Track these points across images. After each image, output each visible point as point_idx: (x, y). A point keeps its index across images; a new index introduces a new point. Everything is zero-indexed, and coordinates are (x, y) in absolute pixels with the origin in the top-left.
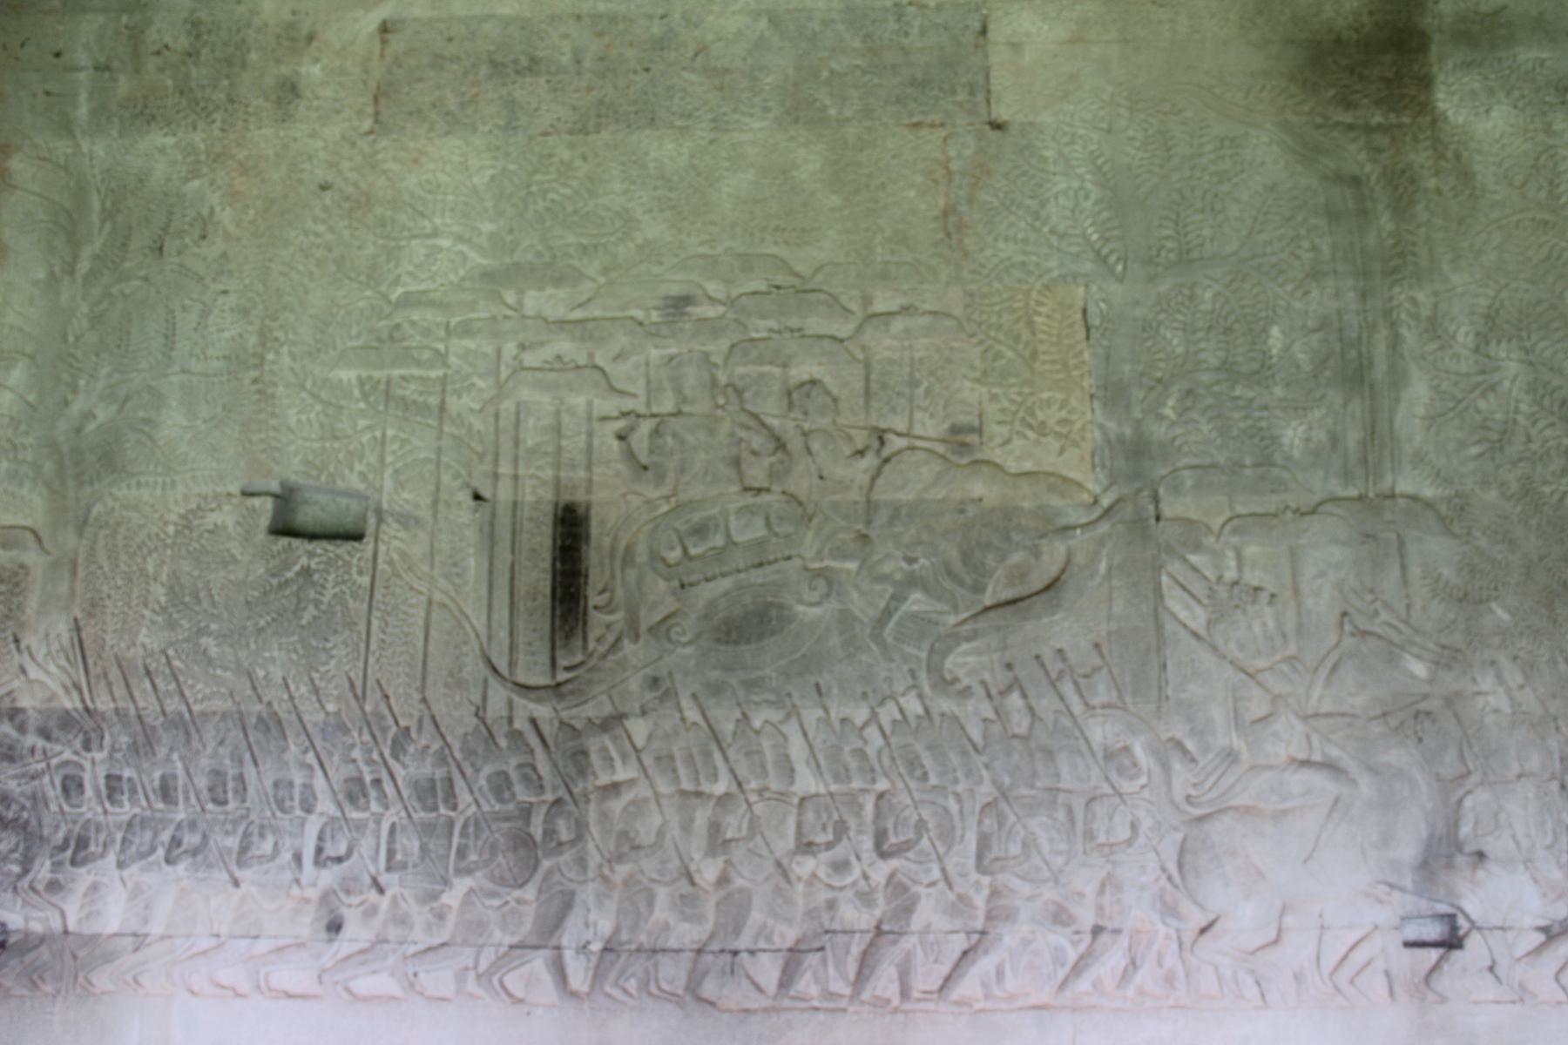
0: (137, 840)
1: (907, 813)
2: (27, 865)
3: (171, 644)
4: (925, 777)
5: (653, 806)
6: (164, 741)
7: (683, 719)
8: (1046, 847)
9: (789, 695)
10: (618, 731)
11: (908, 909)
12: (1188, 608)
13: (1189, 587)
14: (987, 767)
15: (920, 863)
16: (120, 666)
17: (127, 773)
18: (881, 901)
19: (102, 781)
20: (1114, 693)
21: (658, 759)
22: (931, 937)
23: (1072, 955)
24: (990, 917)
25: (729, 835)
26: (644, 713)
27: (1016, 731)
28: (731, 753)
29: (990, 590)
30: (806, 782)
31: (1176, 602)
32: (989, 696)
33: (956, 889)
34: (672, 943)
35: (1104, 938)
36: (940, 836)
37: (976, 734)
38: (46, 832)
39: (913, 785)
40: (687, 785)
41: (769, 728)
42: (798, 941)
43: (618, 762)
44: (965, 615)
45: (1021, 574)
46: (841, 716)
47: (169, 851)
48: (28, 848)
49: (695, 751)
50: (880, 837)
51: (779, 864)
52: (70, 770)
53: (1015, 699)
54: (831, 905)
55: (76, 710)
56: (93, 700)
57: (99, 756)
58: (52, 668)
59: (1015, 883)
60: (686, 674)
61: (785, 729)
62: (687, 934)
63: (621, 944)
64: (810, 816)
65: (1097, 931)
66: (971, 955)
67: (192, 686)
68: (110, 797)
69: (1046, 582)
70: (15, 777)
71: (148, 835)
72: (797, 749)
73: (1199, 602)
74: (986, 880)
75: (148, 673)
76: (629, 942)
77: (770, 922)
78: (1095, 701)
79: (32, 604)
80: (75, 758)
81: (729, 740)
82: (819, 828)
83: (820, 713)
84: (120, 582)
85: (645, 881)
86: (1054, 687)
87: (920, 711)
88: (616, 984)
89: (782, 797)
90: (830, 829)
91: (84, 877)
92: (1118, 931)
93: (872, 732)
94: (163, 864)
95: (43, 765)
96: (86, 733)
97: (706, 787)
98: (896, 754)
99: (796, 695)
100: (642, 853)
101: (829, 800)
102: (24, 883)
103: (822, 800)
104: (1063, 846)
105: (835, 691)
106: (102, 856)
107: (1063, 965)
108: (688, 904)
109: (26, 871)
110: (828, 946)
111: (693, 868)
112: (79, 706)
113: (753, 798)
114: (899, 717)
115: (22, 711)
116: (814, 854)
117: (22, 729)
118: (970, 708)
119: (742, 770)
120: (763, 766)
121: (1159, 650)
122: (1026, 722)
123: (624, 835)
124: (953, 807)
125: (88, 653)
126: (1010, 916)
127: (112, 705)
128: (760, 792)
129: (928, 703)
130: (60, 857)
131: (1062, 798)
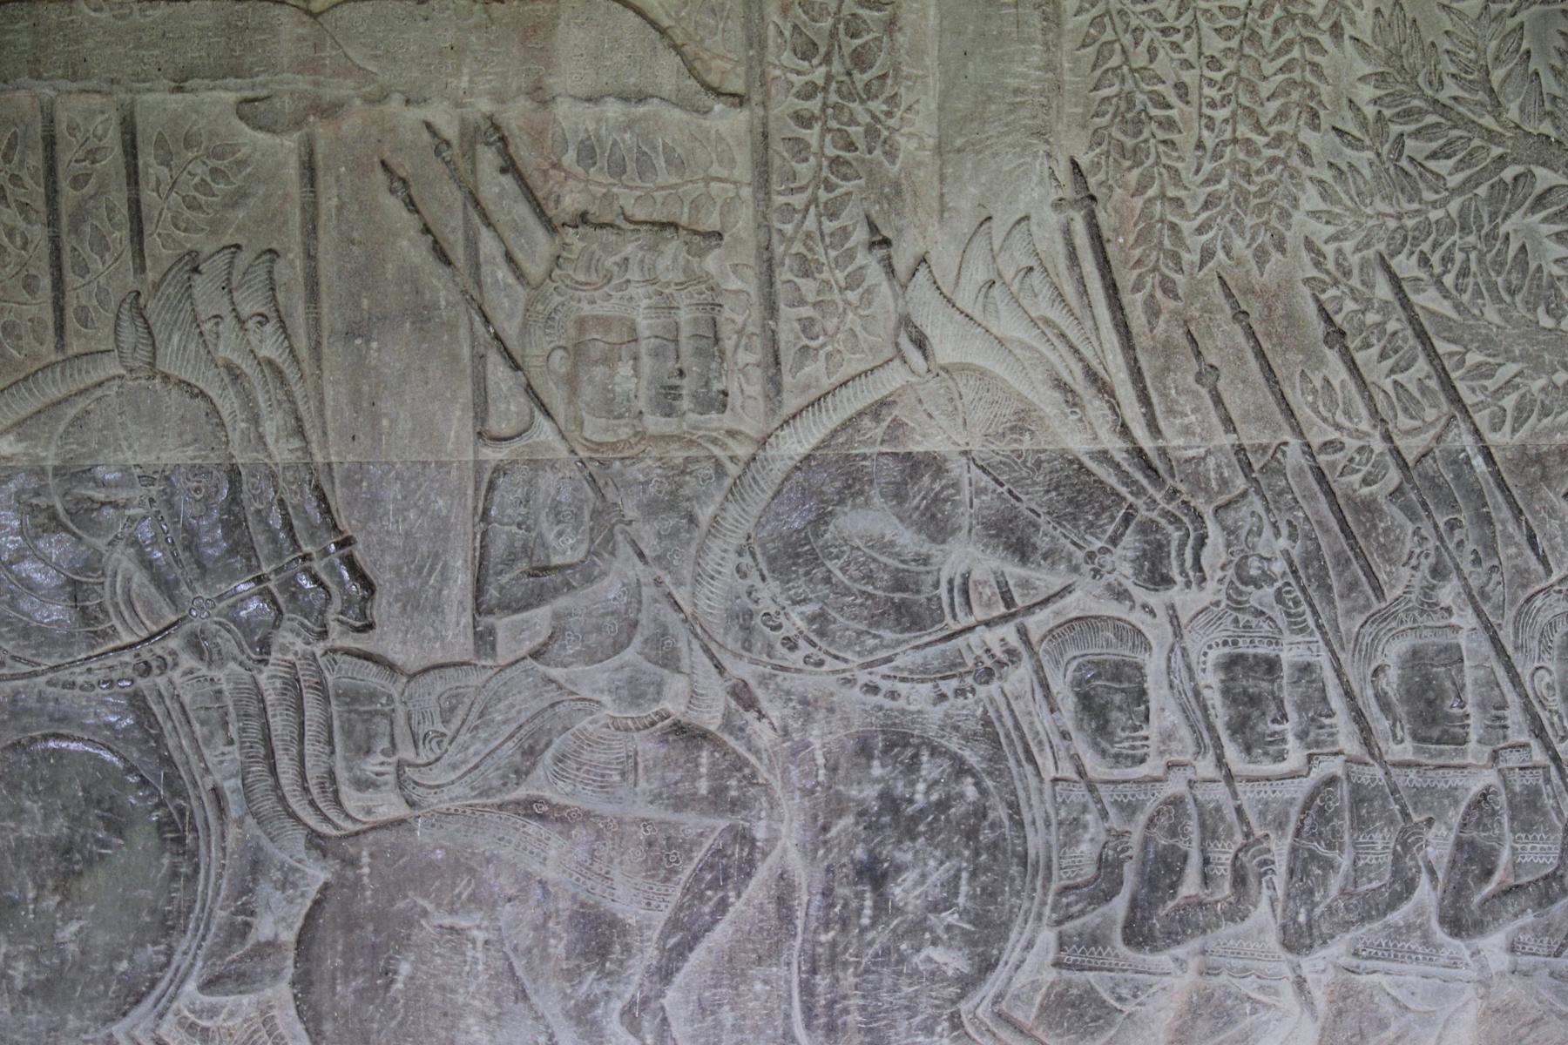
0: (1344, 862)
2: (985, 941)
3: (1403, 240)
6: (1410, 543)
16: (1240, 315)
17: (1290, 653)
19: (1211, 680)
38: (1035, 843)
47: (1457, 892)
48: (990, 894)
52: (1106, 649)
55: (1104, 456)
56: (1154, 429)
57: (1186, 599)
58: (1010, 326)
67: (1482, 372)
68: (1239, 727)
70: (921, 674)
71: (1382, 841)
75: (1336, 336)
79: (916, 131)
80: (1113, 609)
84: (1215, 45)
91: (1171, 976)
94: (1440, 934)
95: (1008, 632)
96: (1147, 528)
102: (978, 1006)
106: (1236, 913)
109: (987, 966)
112: (1116, 446)
115: (934, 464)
117: (936, 524)
125: (1126, 278)
127: (1227, 441)
130: (1093, 918)
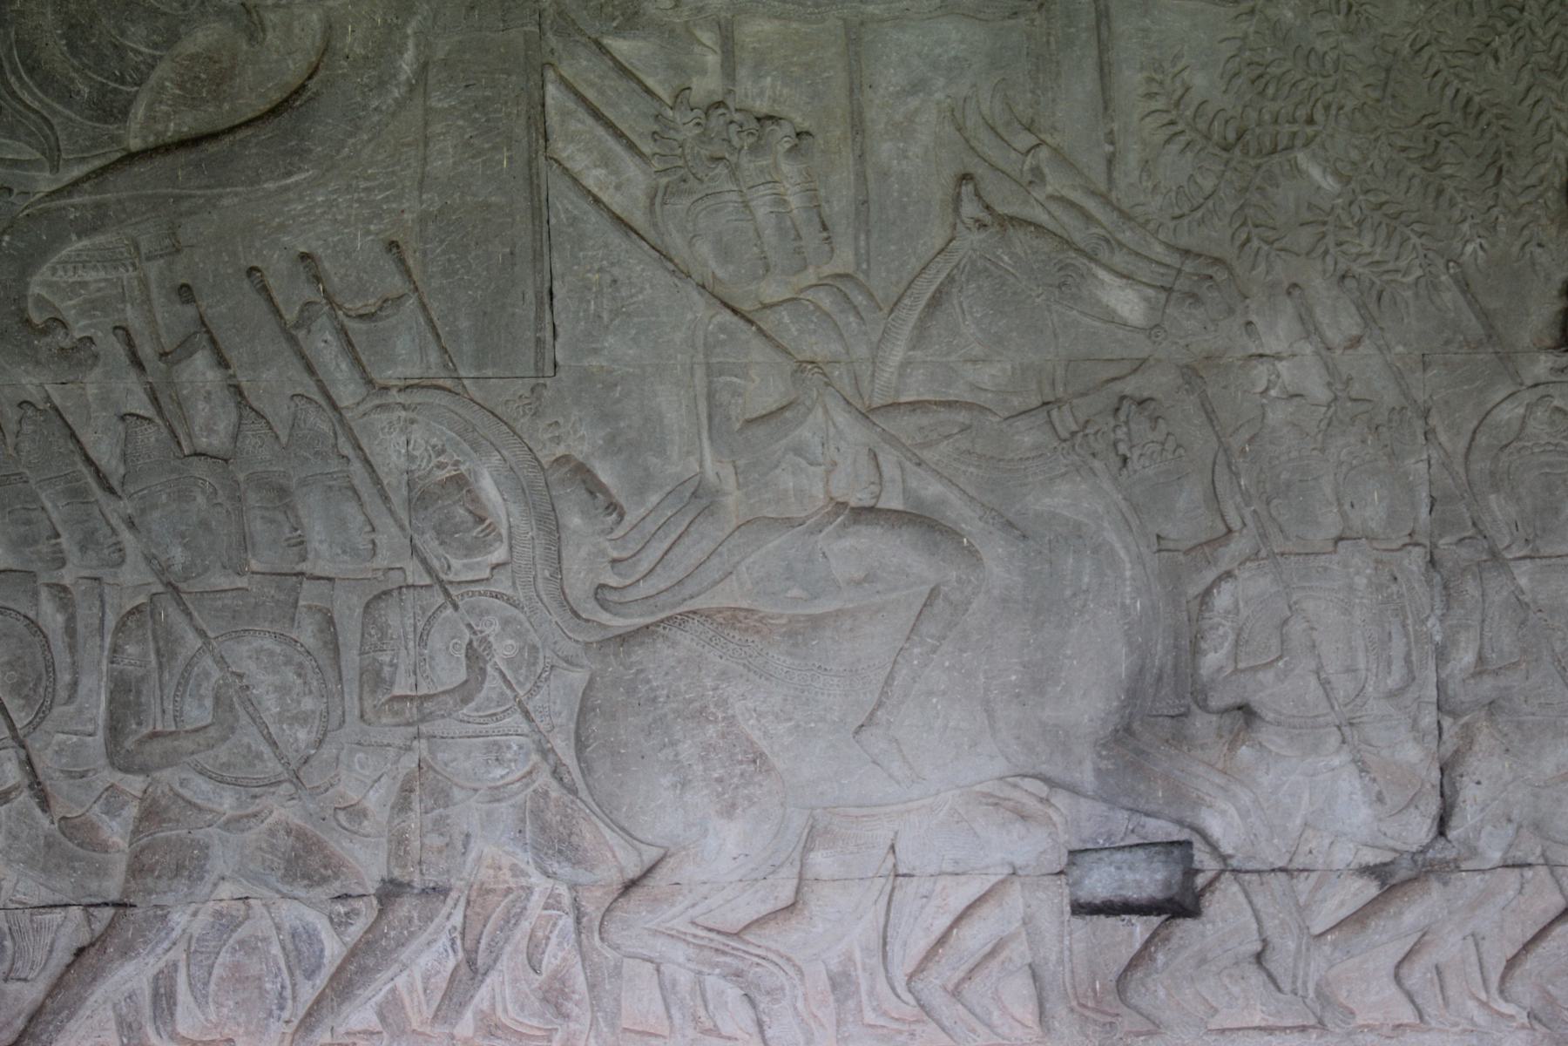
12: (606, 161)
13: (610, 114)
14: (131, 524)
20: (434, 356)
23: (333, 948)
24: (137, 869)
27: (203, 442)
29: (139, 111)
31: (578, 148)
32: (137, 363)
33: (59, 810)
35: (406, 907)
37: (105, 452)
44: (77, 172)
45: (215, 75)
53: (200, 369)
59: (200, 789)
65: (391, 891)
66: (90, 958)
69: (276, 97)
73: (631, 146)
74: (135, 784)
78: (388, 374)
86: (292, 340)
92: (440, 892)
104: (308, 704)
107: (310, 975)
121: (537, 256)
122: (224, 425)
124: (51, 617)
126: (188, 865)
131: (309, 594)
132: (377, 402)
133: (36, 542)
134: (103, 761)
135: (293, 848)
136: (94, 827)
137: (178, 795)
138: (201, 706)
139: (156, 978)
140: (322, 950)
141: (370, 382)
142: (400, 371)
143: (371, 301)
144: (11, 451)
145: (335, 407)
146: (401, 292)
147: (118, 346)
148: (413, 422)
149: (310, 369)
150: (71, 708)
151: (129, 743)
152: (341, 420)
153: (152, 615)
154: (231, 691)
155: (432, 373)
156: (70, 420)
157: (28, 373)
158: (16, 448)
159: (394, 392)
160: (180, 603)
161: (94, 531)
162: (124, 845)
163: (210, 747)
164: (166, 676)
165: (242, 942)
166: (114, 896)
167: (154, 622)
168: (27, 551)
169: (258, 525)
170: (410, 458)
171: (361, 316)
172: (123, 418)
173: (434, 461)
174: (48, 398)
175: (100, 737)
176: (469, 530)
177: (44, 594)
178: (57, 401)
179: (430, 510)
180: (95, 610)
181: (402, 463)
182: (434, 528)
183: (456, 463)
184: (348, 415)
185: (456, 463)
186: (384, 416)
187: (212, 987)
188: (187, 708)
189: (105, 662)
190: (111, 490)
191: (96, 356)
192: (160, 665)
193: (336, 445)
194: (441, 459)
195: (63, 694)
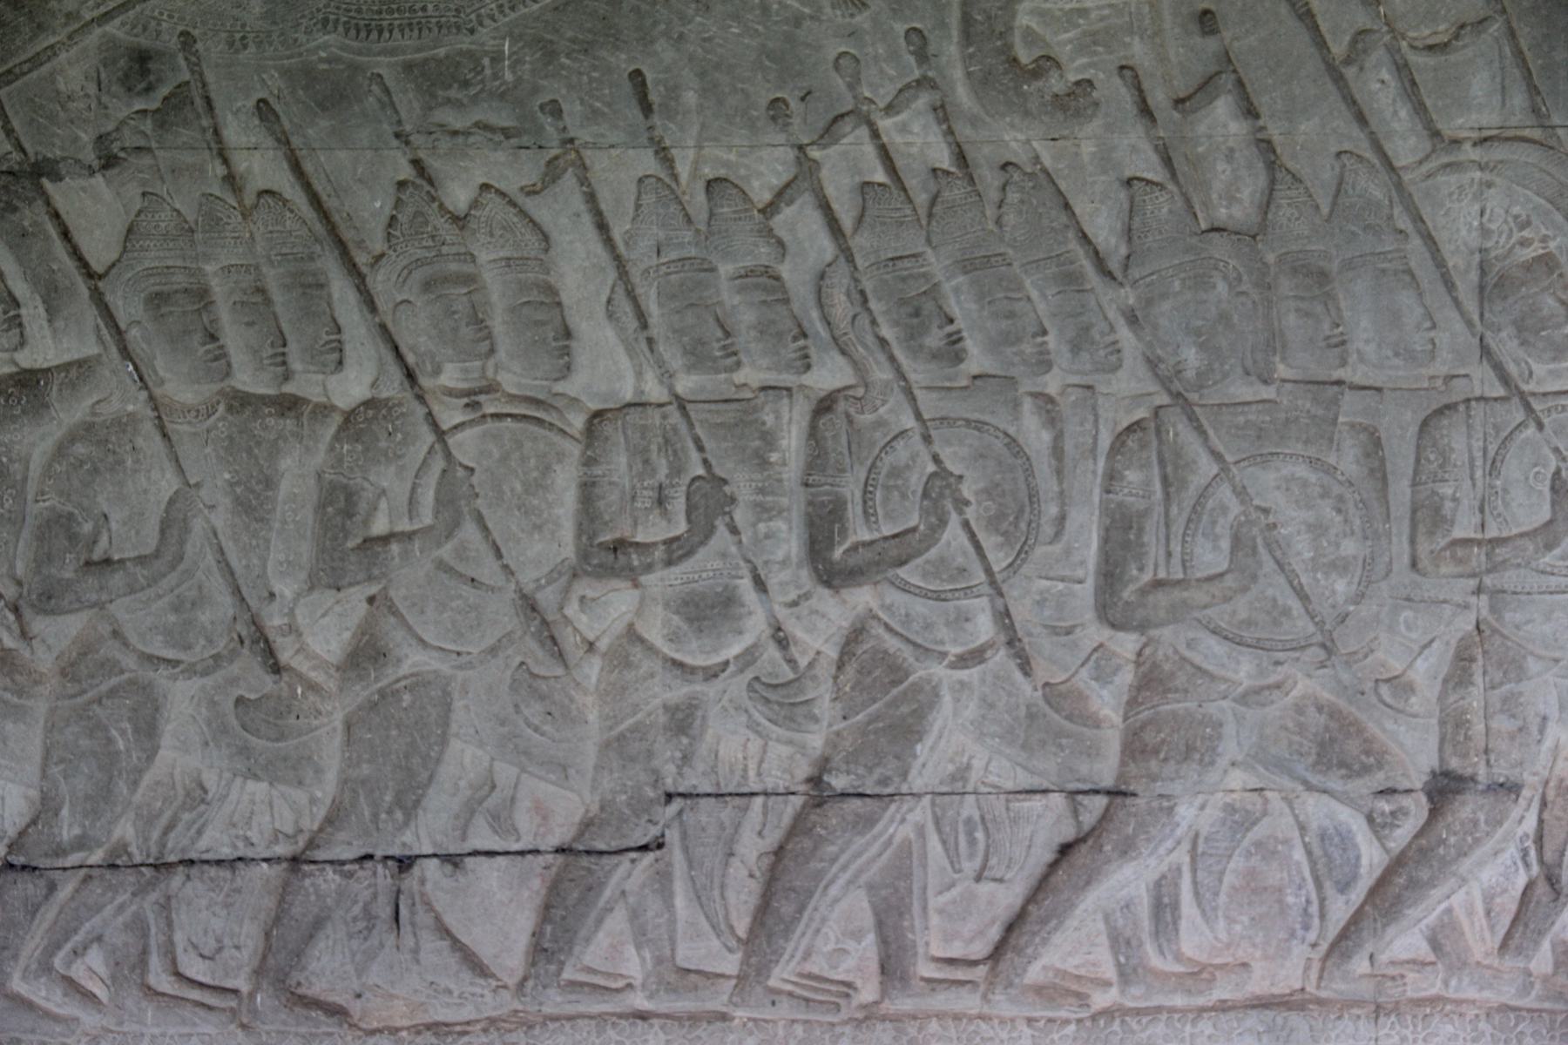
1: (901, 453)
4: (953, 350)
5: (150, 441)
7: (231, 180)
8: (1302, 549)
9: (555, 110)
10: (31, 215)
11: (905, 730)
14: (1132, 319)
15: (938, 596)
18: (825, 707)
20: (1519, 100)
21: (158, 301)
22: (969, 808)
23: (1371, 857)
24: (1135, 747)
25: (380, 526)
26: (109, 162)
28: (380, 282)
30: (607, 368)
32: (1146, 111)
33: (1042, 672)
34: (216, 841)
35: (1467, 808)
36: (994, 523)
37: (1104, 228)
39: (919, 373)
40: (248, 379)
41: (493, 207)
42: (587, 825)
43: (33, 312)
46: (708, 172)
49: (272, 278)
50: (822, 526)
51: (529, 605)
53: (1221, 119)
54: (683, 720)
60: (236, 44)
61: (541, 210)
62: (260, 813)
63: (60, 852)
64: (618, 465)
65: (1445, 788)
72: (579, 270)
74: (1126, 644)
76: (81, 843)
77: (505, 773)
78: (1458, 124)
81: (378, 246)
82: (645, 499)
83: (647, 163)
85: (129, 661)
86: (1339, 80)
87: (944, 159)
88: (46, 968)
89: (536, 411)
90: (678, 505)
92: (1511, 789)
93: (801, 223)
97: (307, 384)
98: (868, 285)
99: (573, 109)
100: (117, 580)
101: (675, 417)
103: (655, 417)
104: (1349, 547)
105: (690, 98)
107: (1344, 887)
108: (261, 727)
110: (672, 836)
111: (274, 621)
113: (450, 415)
114: (880, 176)
116: (632, 576)
118: (1088, 148)
119: (416, 335)
120: (478, 321)
122: (1251, 188)
123: (59, 527)
124: (1035, 434)
126: (1197, 747)
128: (471, 398)
129: (964, 131)
131: (1351, 408)
132: (1446, 159)
133: (1019, 340)
134: (1090, 615)
135: (1327, 728)
136: (1081, 697)
137: (1184, 659)
138: (1216, 548)
139: (1158, 884)
140: (1358, 858)
141: (1435, 134)
142: (1475, 119)
143: (1442, 28)
144: (991, 226)
145: (1390, 167)
146: (1482, 14)
147: (1123, 90)
148: (1489, 185)
149: (1361, 119)
150: (1057, 548)
151: (1128, 594)
152: (1399, 186)
153: (1158, 432)
154: (1255, 531)
155: (1514, 121)
156: (1063, 185)
157: (1012, 126)
158: (998, 222)
159: (1467, 146)
160: (1192, 418)
161: (1087, 329)
162: (1117, 719)
163: (1227, 599)
164: (1174, 510)
165: (1258, 844)
166: (1108, 782)
167: (1161, 442)
168: (1009, 351)
169: (1292, 319)
170: (1485, 232)
171: (1430, 48)
172: (1129, 182)
173: (1516, 236)
174: (1037, 159)
175: (1090, 583)
176: (1559, 326)
177: (1027, 404)
178: (1047, 162)
179: (1511, 300)
180: (1088, 426)
181: (1474, 240)
182: (1514, 323)
183: (1544, 239)
184: (1407, 177)
185: (1544, 239)
186: (1453, 178)
187: (1223, 898)
188: (1198, 550)
189: (1097, 491)
190: (1110, 275)
191: (1096, 104)
192: (1167, 496)
193: (1390, 217)
194: (1526, 233)
195: (1048, 530)
